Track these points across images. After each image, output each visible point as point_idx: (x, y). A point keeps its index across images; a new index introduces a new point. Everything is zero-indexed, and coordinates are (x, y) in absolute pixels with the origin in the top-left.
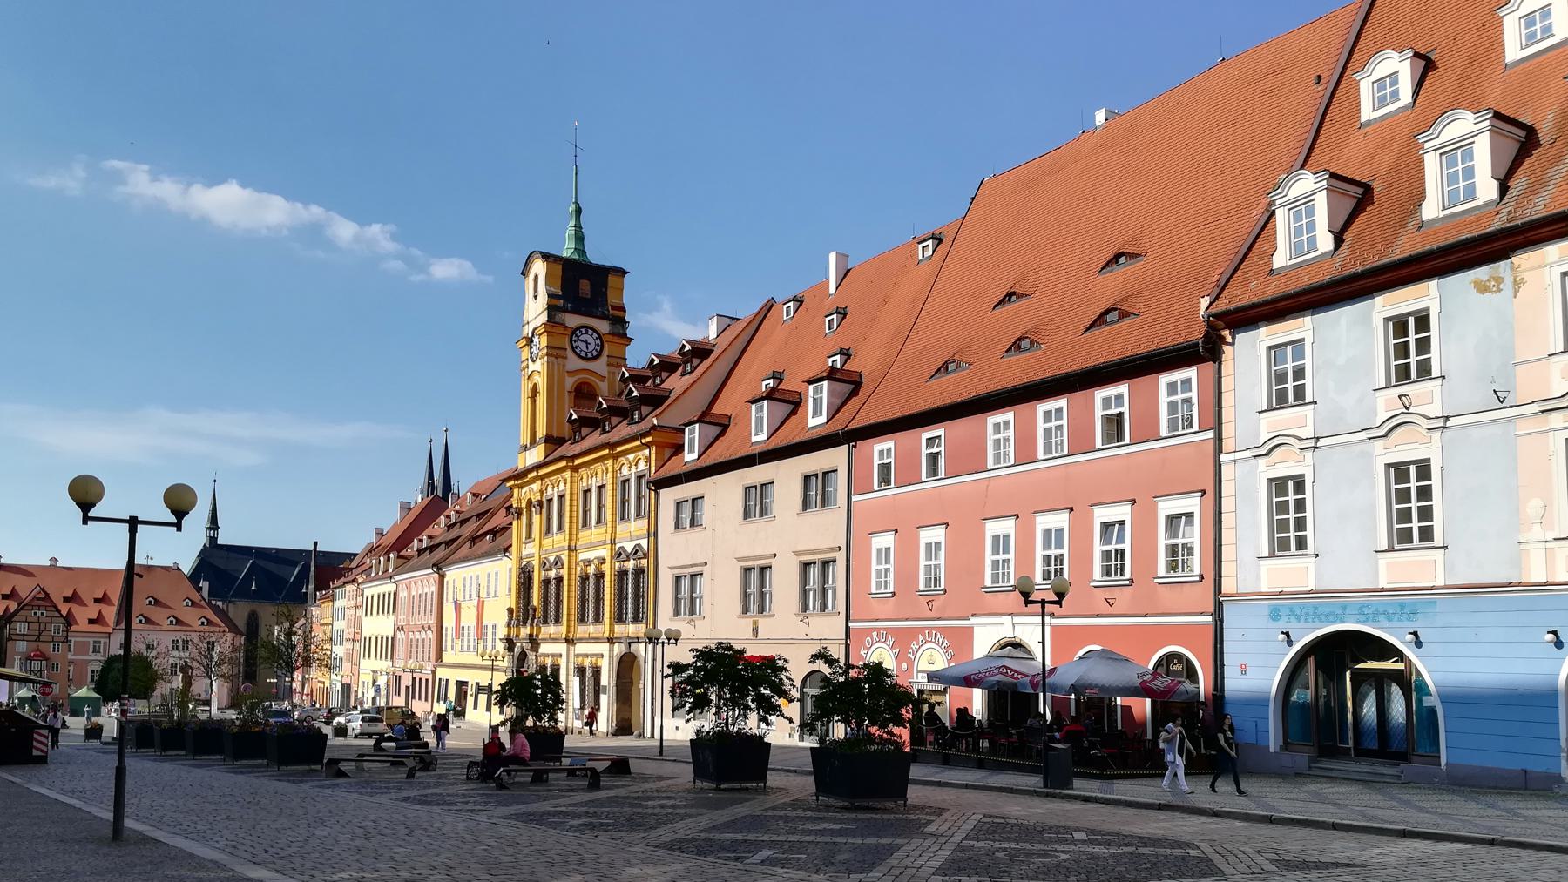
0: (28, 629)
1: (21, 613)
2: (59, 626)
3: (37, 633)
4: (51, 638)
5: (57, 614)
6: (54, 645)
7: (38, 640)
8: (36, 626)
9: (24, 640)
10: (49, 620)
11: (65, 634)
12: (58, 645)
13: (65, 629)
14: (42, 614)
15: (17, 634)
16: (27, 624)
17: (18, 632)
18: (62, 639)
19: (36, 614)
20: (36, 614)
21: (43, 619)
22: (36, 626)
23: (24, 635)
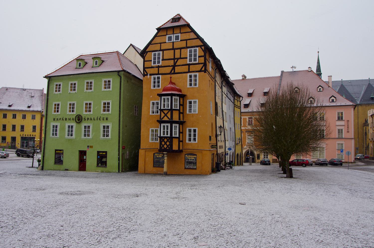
1: (158, 40)
2: (195, 51)
3: (171, 63)
4: (185, 69)
5: (192, 36)
6: (191, 76)
7: (173, 72)
8: (169, 54)
9: (158, 74)
10: (183, 44)
12: (195, 76)
13: (203, 54)
14: (177, 38)
15: (152, 67)
16: (161, 52)
17: (153, 65)
18: (199, 67)
19: (170, 39)
23: (158, 67)
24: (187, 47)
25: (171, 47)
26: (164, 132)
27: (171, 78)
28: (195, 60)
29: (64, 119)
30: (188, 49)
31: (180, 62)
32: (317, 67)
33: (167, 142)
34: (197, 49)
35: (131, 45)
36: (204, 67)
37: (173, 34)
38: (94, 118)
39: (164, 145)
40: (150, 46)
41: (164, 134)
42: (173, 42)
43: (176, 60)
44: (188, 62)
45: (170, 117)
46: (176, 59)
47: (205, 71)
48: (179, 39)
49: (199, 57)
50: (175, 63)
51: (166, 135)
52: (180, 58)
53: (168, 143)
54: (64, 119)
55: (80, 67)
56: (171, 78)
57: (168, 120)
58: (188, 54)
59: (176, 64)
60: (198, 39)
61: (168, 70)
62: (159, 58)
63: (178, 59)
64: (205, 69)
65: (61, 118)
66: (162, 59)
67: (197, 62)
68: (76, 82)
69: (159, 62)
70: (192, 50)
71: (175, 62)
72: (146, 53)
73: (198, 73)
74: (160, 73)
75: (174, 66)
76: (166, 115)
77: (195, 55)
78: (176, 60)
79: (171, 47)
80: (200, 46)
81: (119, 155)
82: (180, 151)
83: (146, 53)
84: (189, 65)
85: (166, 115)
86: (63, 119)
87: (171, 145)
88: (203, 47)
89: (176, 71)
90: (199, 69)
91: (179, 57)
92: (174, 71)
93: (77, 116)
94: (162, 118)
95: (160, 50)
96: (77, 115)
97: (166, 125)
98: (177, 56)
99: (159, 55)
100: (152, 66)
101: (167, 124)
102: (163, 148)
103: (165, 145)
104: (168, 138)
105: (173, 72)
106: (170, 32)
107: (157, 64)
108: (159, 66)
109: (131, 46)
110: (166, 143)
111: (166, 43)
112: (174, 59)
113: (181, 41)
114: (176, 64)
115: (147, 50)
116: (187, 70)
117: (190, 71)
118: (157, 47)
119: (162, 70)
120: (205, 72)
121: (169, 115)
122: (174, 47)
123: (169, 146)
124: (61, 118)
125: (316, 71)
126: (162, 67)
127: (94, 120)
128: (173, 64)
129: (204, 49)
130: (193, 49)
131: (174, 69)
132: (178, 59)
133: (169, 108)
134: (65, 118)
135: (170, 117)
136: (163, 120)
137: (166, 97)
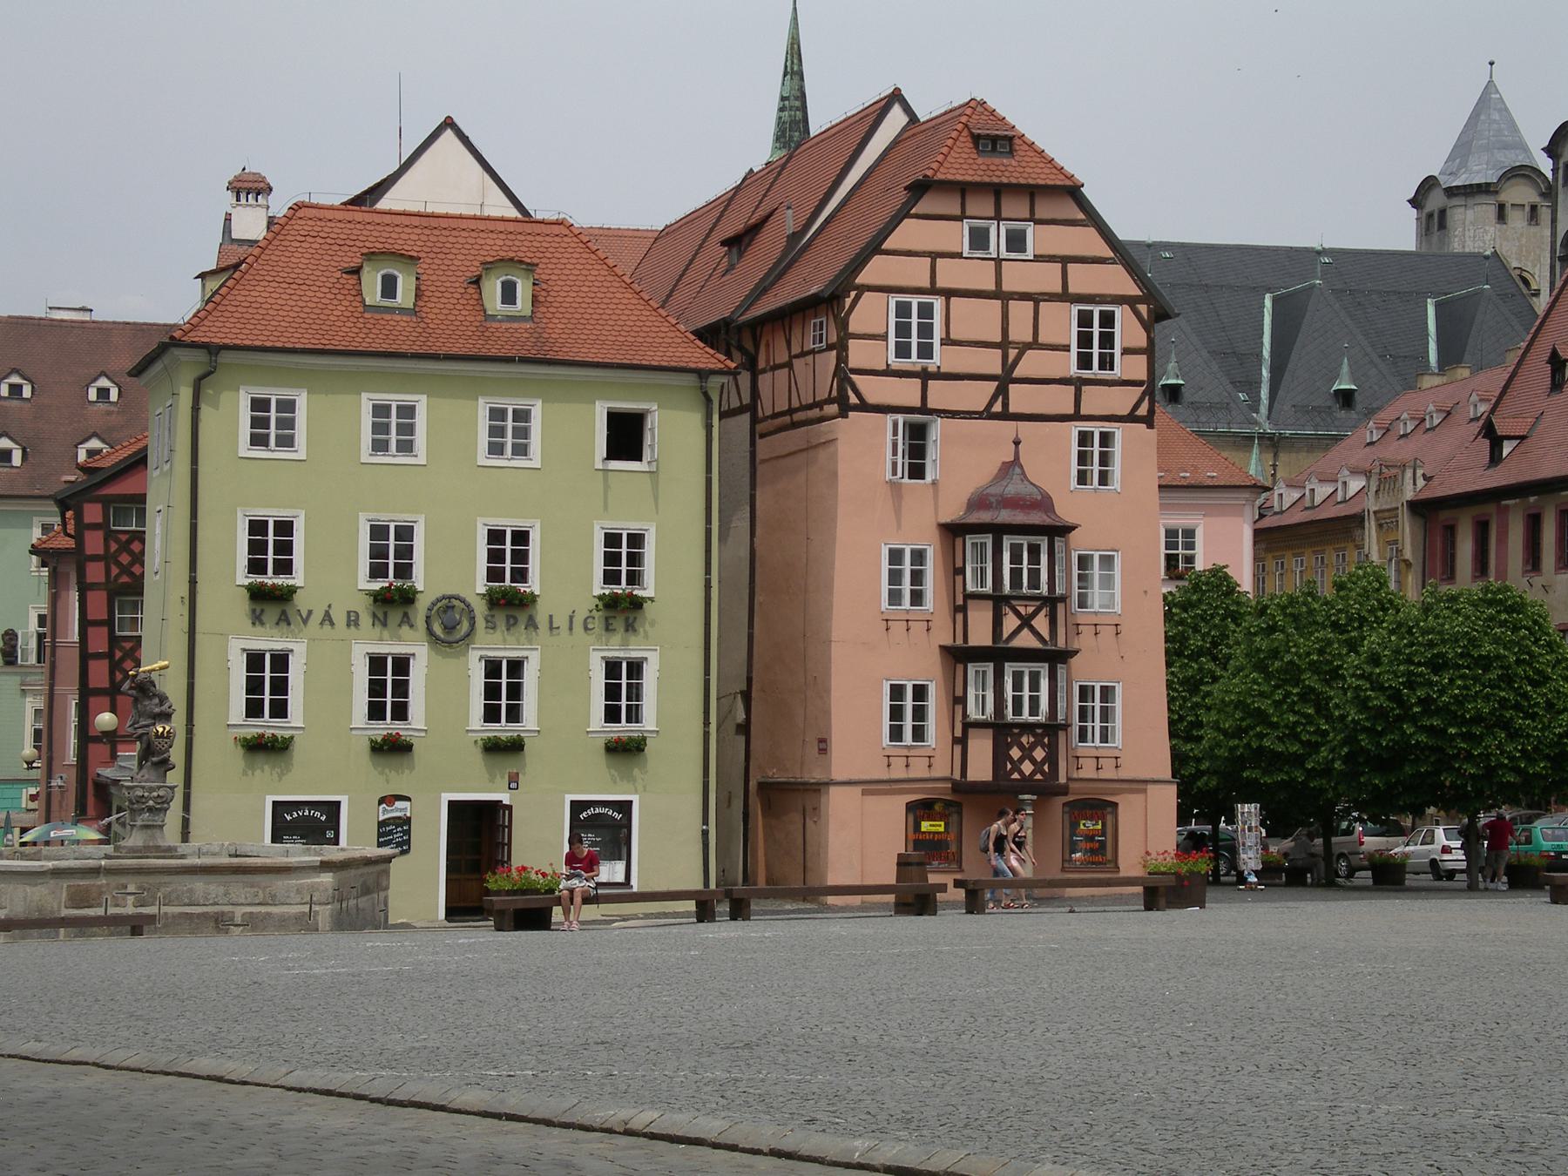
0: (947, 341)
1: (909, 234)
2: (1108, 320)
3: (991, 362)
4: (1061, 399)
6: (1085, 438)
10: (1047, 278)
11: (1136, 368)
12: (1106, 439)
13: (1141, 340)
14: (1016, 241)
15: (889, 372)
16: (938, 303)
18: (1122, 400)
19: (979, 239)
20: (979, 239)
21: (1018, 277)
22: (979, 319)
23: (925, 376)
24: (1065, 296)
25: (992, 287)
26: (1017, 701)
27: (1017, 443)
28: (1107, 362)
29: (339, 617)
30: (1075, 309)
31: (1031, 365)
32: (781, 109)
33: (1033, 747)
34: (1119, 312)
35: (449, 123)
36: (1147, 398)
37: (998, 217)
38: (551, 616)
39: (1021, 760)
40: (877, 260)
41: (1018, 709)
42: (998, 261)
43: (1013, 353)
44: (1073, 370)
45: (1045, 633)
46: (1016, 344)
47: (1148, 421)
48: (1024, 250)
49: (1126, 351)
50: (1008, 367)
51: (1025, 716)
52: (1035, 344)
53: (1039, 754)
54: (339, 617)
55: (388, 303)
56: (1017, 443)
57: (1036, 644)
58: (1075, 329)
59: (1017, 373)
60: (1115, 263)
61: (978, 395)
62: (926, 331)
63: (1025, 347)
64: (1151, 411)
65: (310, 612)
66: (944, 336)
67: (1117, 372)
68: (422, 403)
69: (926, 351)
70: (1092, 311)
71: (1010, 360)
72: (853, 294)
73: (1117, 424)
74: (930, 405)
75: (1005, 381)
76: (1026, 622)
77: (1107, 340)
78: (1013, 353)
79: (992, 287)
80: (1130, 301)
81: (705, 821)
82: (1064, 791)
83: (853, 294)
84: (1079, 384)
85: (1026, 622)
86: (328, 618)
87: (1052, 758)
88: (1143, 309)
89: (1012, 409)
90: (1126, 412)
91: (1030, 339)
92: (1005, 405)
93: (439, 605)
94: (1005, 636)
95: (933, 290)
96: (439, 600)
97: (1026, 668)
98: (1020, 331)
99: (926, 311)
100: (888, 365)
101: (1035, 666)
102: (1016, 776)
103: (1027, 761)
104: (1039, 731)
105: (997, 408)
106: (981, 206)
107: (914, 361)
108: (925, 370)
109: (449, 134)
110: (1027, 754)
111: (959, 255)
112: (1004, 345)
113: (1038, 258)
114: (1017, 373)
115: (859, 280)
116: (1071, 411)
117: (1083, 411)
118: (916, 272)
119: (940, 394)
120: (1150, 426)
121: (1041, 623)
122: (1006, 287)
123: (1046, 768)
124: (310, 612)
125: (777, 139)
126: (940, 376)
127: (551, 628)
128: (998, 370)
129: (1145, 316)
130: (1096, 310)
131: (1002, 391)
132: (1025, 347)
133: (1044, 589)
134: (349, 613)
135: (1045, 633)
136: (1010, 645)
137: (1024, 541)
